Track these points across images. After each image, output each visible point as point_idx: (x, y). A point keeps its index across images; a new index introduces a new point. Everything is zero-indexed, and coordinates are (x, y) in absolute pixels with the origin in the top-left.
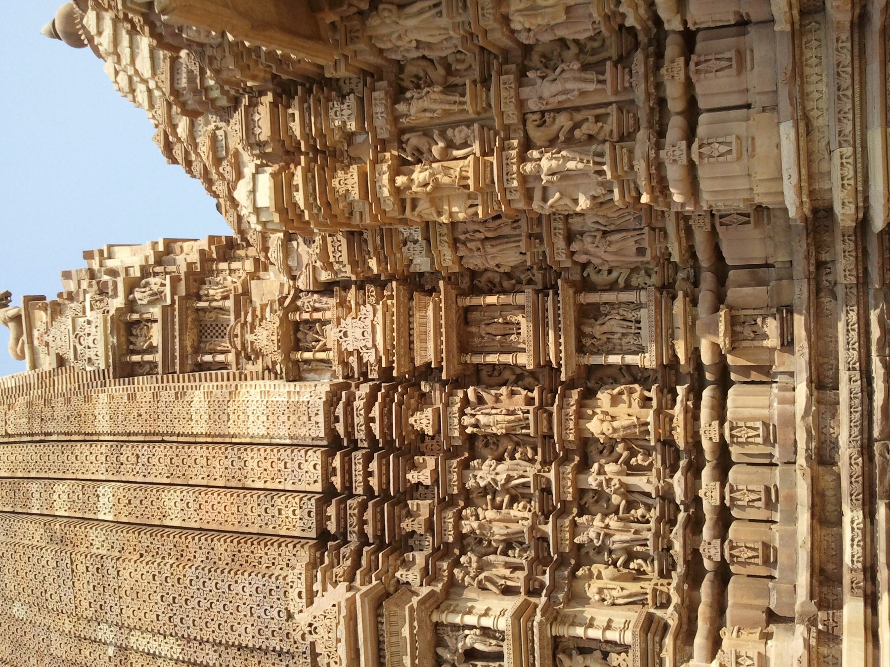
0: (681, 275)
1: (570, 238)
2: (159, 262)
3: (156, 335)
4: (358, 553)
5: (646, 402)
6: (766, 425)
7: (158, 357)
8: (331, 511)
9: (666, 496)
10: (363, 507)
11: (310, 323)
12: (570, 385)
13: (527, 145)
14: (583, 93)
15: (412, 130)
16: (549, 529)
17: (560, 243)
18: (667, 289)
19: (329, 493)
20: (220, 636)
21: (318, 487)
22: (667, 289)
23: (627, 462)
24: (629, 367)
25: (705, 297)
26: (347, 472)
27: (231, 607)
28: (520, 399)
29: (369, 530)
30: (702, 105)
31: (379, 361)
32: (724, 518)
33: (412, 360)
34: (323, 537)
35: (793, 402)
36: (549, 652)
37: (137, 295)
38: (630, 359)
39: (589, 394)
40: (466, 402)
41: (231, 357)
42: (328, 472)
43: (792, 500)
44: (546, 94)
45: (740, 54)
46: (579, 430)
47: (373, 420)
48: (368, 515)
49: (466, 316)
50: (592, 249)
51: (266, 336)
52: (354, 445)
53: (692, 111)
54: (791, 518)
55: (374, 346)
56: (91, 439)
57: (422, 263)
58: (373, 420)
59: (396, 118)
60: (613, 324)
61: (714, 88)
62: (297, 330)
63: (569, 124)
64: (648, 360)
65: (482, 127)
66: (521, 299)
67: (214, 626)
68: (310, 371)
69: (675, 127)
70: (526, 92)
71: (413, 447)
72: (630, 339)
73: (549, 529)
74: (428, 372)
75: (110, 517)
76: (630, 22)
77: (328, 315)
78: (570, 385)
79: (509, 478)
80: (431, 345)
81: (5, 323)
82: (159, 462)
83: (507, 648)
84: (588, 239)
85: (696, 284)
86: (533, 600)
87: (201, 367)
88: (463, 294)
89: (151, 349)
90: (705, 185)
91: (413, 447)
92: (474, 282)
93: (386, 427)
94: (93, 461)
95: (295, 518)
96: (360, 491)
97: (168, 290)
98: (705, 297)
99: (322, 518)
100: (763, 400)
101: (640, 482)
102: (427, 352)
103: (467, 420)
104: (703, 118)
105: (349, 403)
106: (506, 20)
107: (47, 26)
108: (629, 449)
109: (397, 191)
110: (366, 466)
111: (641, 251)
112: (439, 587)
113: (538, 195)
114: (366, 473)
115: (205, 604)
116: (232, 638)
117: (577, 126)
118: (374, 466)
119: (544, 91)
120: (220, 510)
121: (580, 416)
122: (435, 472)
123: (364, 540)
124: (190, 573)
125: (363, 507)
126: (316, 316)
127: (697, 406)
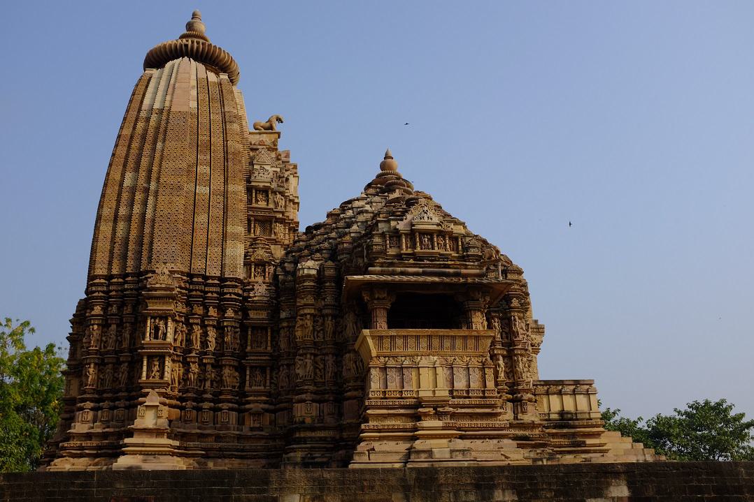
0: (274, 400)
1: (288, 366)
2: (290, 200)
3: (262, 204)
4: (185, 289)
5: (234, 387)
6: (227, 422)
7: (254, 205)
8: (200, 280)
9: (205, 392)
10: (201, 291)
11: (264, 271)
12: (240, 363)
13: (316, 355)
14: (328, 372)
15: (324, 320)
16: (193, 354)
17: (286, 362)
18: (269, 395)
19: (205, 278)
20: (156, 235)
21: (208, 274)
22: (269, 395)
23: (214, 381)
24: (245, 382)
25: (266, 406)
26: (213, 285)
27: (167, 241)
28: (237, 346)
29: (194, 293)
30: (321, 405)
31: (250, 297)
32: (199, 409)
33: (250, 310)
34: (190, 275)
35: (234, 430)
36: (161, 354)
37: (279, 196)
38: (247, 383)
39: (236, 369)
40: (235, 327)
41: (252, 236)
42: (213, 278)
43: (205, 429)
44: (329, 362)
45: (333, 414)
46: (225, 365)
47: (230, 295)
48: (199, 293)
49: (264, 329)
50: (283, 373)
51: (261, 253)
52: (222, 287)
53: (319, 402)
54: (199, 428)
55: (255, 296)
56: (226, 182)
57: (283, 315)
58: (230, 295)
59: (327, 315)
60: (259, 378)
61: (327, 408)
62: (262, 266)
63: (320, 368)
64: (247, 388)
65: (322, 342)
66: (269, 348)
67: (160, 233)
68: (247, 269)
69: (318, 397)
70: (330, 356)
71: (222, 310)
72: (254, 383)
73: (193, 354)
74: (246, 316)
75: (197, 191)
76: (345, 386)
77: (267, 279)
78: (240, 363)
79: (210, 342)
80: (255, 317)
81: (269, 121)
82: (217, 212)
83: (160, 341)
84: (287, 371)
85: (271, 404)
86: (173, 348)
87: (249, 220)
88: (272, 328)
89: (257, 201)
90: (299, 405)
91: (222, 310)
92: (276, 333)
93: (228, 300)
94: (217, 183)
95: (198, 265)
96: (206, 289)
97: (279, 209)
98: (266, 406)
99: (198, 276)
100: (234, 423)
101: (208, 384)
102: (252, 314)
103: (229, 329)
104: (318, 405)
105: (236, 287)
106: (349, 352)
107: (391, 154)
108: (219, 381)
109: (306, 314)
110: (215, 292)
111: (282, 387)
112: (177, 318)
113: (302, 358)
114: (212, 293)
115: (168, 231)
116: (155, 240)
117: (320, 370)
118: (215, 295)
119: (330, 360)
120: (200, 238)
121: (230, 366)
122: (212, 316)
123: (191, 291)
124: (180, 226)
125: (201, 291)
126: (267, 273)
127: (232, 403)
